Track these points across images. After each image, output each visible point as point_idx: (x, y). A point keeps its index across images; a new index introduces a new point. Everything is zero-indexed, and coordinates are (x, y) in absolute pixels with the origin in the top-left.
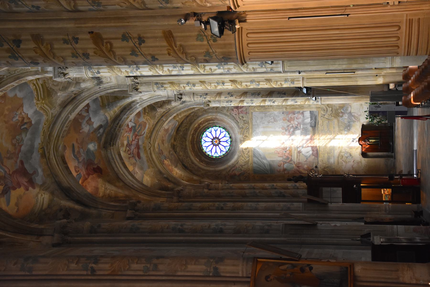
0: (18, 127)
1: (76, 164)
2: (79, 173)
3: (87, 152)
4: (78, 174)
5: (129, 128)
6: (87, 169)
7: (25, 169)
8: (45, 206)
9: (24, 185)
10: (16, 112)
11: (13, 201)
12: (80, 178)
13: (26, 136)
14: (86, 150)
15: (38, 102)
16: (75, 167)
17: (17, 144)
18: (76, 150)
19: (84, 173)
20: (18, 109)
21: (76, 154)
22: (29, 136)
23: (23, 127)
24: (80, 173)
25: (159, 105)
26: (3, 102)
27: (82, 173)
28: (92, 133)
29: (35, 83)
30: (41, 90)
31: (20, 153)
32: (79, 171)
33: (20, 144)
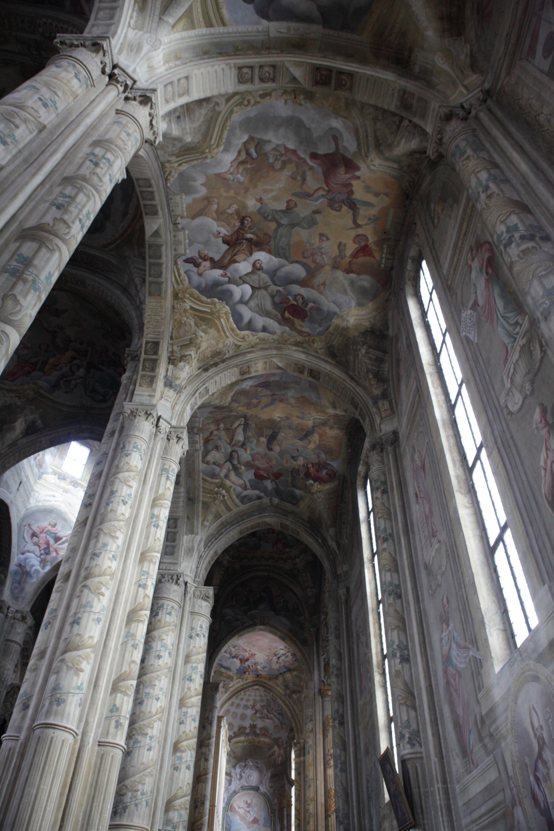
0: (253, 166)
7: (327, 156)
8: (395, 166)
9: (349, 179)
10: (229, 180)
11: (370, 198)
13: (269, 141)
15: (209, 156)
17: (284, 158)
20: (225, 179)
22: (270, 136)
23: (254, 155)
26: (216, 200)
29: (176, 164)
30: (187, 156)
31: (299, 152)
33: (283, 152)
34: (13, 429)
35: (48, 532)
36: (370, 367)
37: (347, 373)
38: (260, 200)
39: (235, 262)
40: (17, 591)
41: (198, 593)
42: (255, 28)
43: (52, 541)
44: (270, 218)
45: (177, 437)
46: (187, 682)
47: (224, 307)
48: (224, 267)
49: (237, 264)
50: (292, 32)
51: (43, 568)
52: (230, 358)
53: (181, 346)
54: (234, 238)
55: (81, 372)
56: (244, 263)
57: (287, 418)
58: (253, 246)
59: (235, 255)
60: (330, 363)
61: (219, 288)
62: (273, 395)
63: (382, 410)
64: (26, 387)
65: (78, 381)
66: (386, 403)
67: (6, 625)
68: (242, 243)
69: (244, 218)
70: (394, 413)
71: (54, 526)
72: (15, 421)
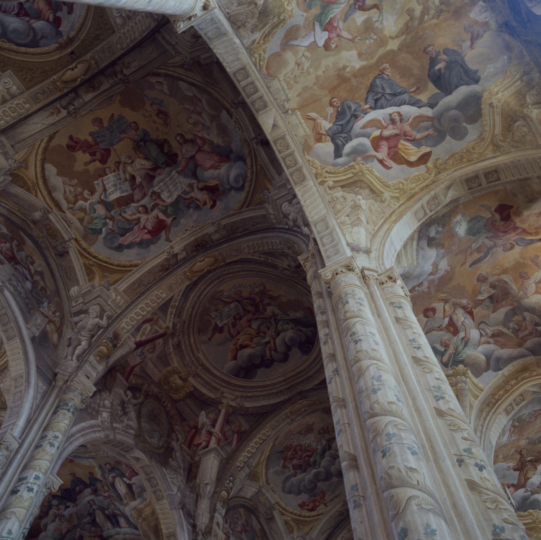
1: (500, 249)
2: (514, 243)
3: (474, 235)
4: (517, 244)
5: (331, 36)
6: (505, 232)
12: (523, 239)
14: (471, 237)
16: (506, 250)
17: (535, 415)
18: (476, 256)
19: (513, 234)
21: (482, 254)
24: (514, 241)
25: (251, 8)
27: (514, 239)
28: (443, 246)
32: (511, 244)
38: (528, 438)
39: (529, 478)
42: (497, 378)
44: (537, 442)
47: (539, 513)
48: (523, 486)
49: (530, 480)
50: (516, 366)
54: (520, 465)
56: (535, 476)
58: (535, 463)
59: (526, 475)
61: (528, 501)
68: (526, 465)
69: (521, 451)
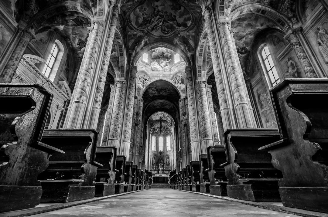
34: (141, 44)
35: (143, 78)
36: (289, 7)
37: (276, 11)
40: (138, 94)
41: (208, 87)
43: (144, 80)
45: (233, 32)
46: (211, 109)
51: (143, 88)
52: (238, 7)
53: (228, 2)
55: (161, 23)
57: (238, 32)
60: (270, 8)
62: (239, 23)
63: (293, 21)
64: (145, 29)
65: (160, 27)
66: (295, 19)
67: (138, 102)
70: (299, 21)
71: (144, 76)
72: (142, 41)
